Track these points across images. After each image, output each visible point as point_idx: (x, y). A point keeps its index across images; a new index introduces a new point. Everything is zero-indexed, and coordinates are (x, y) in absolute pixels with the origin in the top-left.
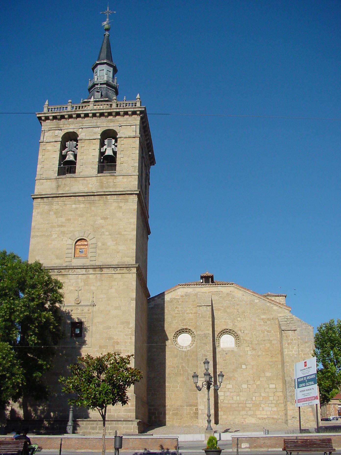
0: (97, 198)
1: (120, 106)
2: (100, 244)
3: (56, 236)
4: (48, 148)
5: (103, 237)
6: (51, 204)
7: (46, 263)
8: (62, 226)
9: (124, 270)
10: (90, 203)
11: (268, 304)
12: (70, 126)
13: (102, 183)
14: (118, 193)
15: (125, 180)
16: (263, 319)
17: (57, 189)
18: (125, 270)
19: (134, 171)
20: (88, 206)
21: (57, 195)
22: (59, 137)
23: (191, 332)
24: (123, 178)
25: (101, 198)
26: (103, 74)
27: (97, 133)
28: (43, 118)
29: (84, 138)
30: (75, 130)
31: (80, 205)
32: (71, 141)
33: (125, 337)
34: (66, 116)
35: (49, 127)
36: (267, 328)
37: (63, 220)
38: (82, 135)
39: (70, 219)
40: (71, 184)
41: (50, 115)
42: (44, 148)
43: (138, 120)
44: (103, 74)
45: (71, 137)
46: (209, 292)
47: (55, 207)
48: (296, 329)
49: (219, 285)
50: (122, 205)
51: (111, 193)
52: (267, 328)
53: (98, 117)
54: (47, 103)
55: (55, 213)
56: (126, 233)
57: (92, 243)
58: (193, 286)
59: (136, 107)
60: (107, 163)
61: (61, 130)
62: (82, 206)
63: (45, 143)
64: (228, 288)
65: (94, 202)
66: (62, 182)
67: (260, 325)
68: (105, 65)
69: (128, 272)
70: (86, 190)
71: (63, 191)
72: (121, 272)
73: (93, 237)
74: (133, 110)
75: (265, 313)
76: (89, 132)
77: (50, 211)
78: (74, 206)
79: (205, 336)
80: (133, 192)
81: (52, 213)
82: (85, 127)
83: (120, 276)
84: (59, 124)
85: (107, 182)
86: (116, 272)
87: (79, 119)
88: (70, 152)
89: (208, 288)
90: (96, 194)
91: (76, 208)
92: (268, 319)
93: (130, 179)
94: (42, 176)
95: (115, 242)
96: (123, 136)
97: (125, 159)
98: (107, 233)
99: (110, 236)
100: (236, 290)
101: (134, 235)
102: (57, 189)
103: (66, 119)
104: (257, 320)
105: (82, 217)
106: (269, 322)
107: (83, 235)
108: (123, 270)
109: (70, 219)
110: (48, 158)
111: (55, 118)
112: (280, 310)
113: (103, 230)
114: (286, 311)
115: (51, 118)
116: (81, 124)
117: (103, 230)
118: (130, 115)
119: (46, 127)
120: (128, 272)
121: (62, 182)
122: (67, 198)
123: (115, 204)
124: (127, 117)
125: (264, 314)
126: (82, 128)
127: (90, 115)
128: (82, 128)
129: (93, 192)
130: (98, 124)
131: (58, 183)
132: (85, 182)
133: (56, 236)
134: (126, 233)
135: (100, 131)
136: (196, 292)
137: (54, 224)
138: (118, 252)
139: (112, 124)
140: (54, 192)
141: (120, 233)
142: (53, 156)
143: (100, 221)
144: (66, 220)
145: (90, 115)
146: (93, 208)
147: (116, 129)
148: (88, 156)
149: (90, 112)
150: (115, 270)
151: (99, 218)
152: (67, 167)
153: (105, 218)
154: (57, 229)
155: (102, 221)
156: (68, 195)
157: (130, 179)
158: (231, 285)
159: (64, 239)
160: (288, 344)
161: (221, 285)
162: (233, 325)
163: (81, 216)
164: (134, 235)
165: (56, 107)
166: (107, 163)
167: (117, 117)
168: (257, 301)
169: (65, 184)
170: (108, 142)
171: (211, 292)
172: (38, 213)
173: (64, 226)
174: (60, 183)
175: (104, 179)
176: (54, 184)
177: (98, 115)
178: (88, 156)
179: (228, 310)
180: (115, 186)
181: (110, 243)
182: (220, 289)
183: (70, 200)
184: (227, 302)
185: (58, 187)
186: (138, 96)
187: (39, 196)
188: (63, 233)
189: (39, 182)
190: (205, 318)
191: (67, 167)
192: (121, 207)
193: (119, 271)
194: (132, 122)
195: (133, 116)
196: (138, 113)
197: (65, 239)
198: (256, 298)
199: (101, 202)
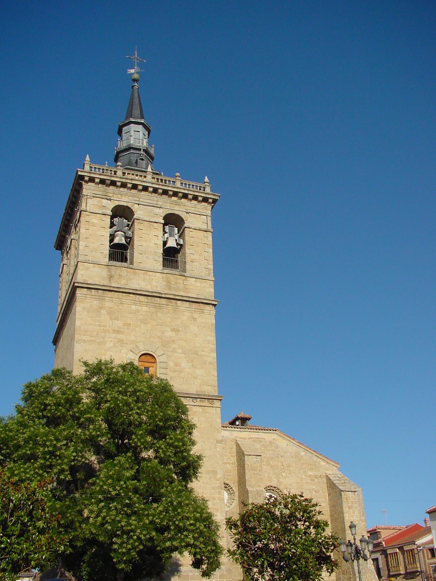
0: (163, 301)
1: (200, 189)
2: (171, 364)
3: (112, 345)
4: (93, 221)
5: (175, 354)
6: (102, 299)
7: (178, 386)
8: (118, 332)
9: (205, 402)
10: (154, 307)
11: (315, 458)
12: (125, 198)
13: (168, 282)
14: (191, 300)
15: (198, 284)
16: (310, 476)
17: (110, 281)
18: (206, 403)
19: (209, 275)
20: (153, 310)
21: (112, 289)
22: (109, 209)
23: (229, 488)
24: (195, 281)
25: (170, 302)
26: (136, 136)
27: (159, 215)
28: (87, 179)
29: (142, 217)
30: (129, 205)
31: (143, 307)
32: (121, 217)
33: (213, 490)
34: (119, 184)
35: (93, 192)
36: (314, 487)
37: (120, 323)
38: (139, 212)
39: (130, 324)
40: (123, 276)
41: (97, 176)
42: (87, 219)
43: (208, 210)
44: (136, 136)
45: (122, 213)
46: (249, 438)
47: (107, 304)
48: (355, 490)
49: (260, 431)
50: (196, 315)
51: (183, 298)
52: (314, 487)
53: (159, 194)
54: (88, 158)
55: (109, 313)
56: (203, 353)
57: (162, 361)
58: (255, 431)
59: (205, 192)
60: (171, 256)
61: (110, 200)
62: (145, 308)
63: (88, 214)
64: (270, 434)
65: (160, 306)
66: (115, 272)
67: (307, 483)
68: (141, 126)
69: (210, 405)
70: (149, 288)
71: (118, 283)
72: (202, 404)
73: (162, 353)
74: (204, 195)
75: (312, 469)
76: (149, 211)
77: (101, 308)
78: (133, 307)
79: (258, 494)
80: (210, 302)
81: (103, 312)
82: (143, 203)
83: (200, 409)
84: (107, 191)
85: (176, 283)
86: (195, 404)
87: (134, 191)
88: (120, 233)
89: (248, 433)
90: (163, 296)
91: (137, 311)
92: (316, 477)
93: (205, 284)
94: (87, 258)
95: (191, 364)
96: (191, 226)
97: (196, 257)
98: (180, 351)
99: (183, 355)
100: (279, 438)
101: (214, 358)
102: (110, 281)
103: (117, 186)
104: (304, 477)
105: (146, 324)
106: (316, 480)
107: (153, 350)
108: (204, 402)
109: (130, 325)
110: (93, 233)
111: (103, 182)
112: (328, 466)
113: (174, 346)
114: (334, 468)
115: (97, 180)
116: (137, 199)
117: (174, 346)
118: (199, 202)
119: (89, 191)
120: (210, 405)
121: (115, 272)
122: (124, 294)
123: (188, 314)
124: (196, 202)
125: (311, 469)
126: (139, 204)
127: (151, 189)
128: (139, 204)
129: (160, 293)
130: (160, 203)
131: (110, 271)
132: (147, 277)
133: (112, 345)
134: (203, 353)
135: (162, 213)
136: (233, 437)
137: (108, 328)
138: (195, 378)
139: (176, 208)
140: (106, 283)
141: (196, 353)
142: (100, 233)
143: (170, 334)
144: (125, 324)
145: (151, 189)
146: (159, 314)
147: (135, 208)
148: (149, 241)
149: (151, 185)
150: (195, 401)
151: (168, 329)
152: (120, 252)
153: (177, 331)
154: (113, 335)
155: (173, 334)
156: (127, 291)
157: (204, 284)
158: (274, 432)
159: (122, 351)
160: (349, 508)
161: (263, 431)
162: (278, 481)
163: (145, 322)
164: (214, 358)
165: (102, 168)
166: (171, 256)
167: (183, 200)
168: (302, 454)
169: (119, 275)
170: (169, 230)
171: (251, 438)
172: (84, 308)
173: (122, 333)
174: (113, 273)
175: (172, 278)
176: (104, 272)
177: (160, 191)
178: (149, 241)
179: (271, 462)
180: (186, 289)
181: (184, 364)
182: (262, 435)
183: (128, 298)
184: (270, 452)
185: (111, 277)
186: (206, 179)
187: (86, 286)
188: (121, 342)
189: (83, 265)
190: (254, 470)
191: (120, 252)
192: (195, 319)
193: (198, 402)
194: (202, 211)
195: (203, 204)
196: (211, 201)
197: (124, 350)
198: (301, 450)
199: (170, 308)
